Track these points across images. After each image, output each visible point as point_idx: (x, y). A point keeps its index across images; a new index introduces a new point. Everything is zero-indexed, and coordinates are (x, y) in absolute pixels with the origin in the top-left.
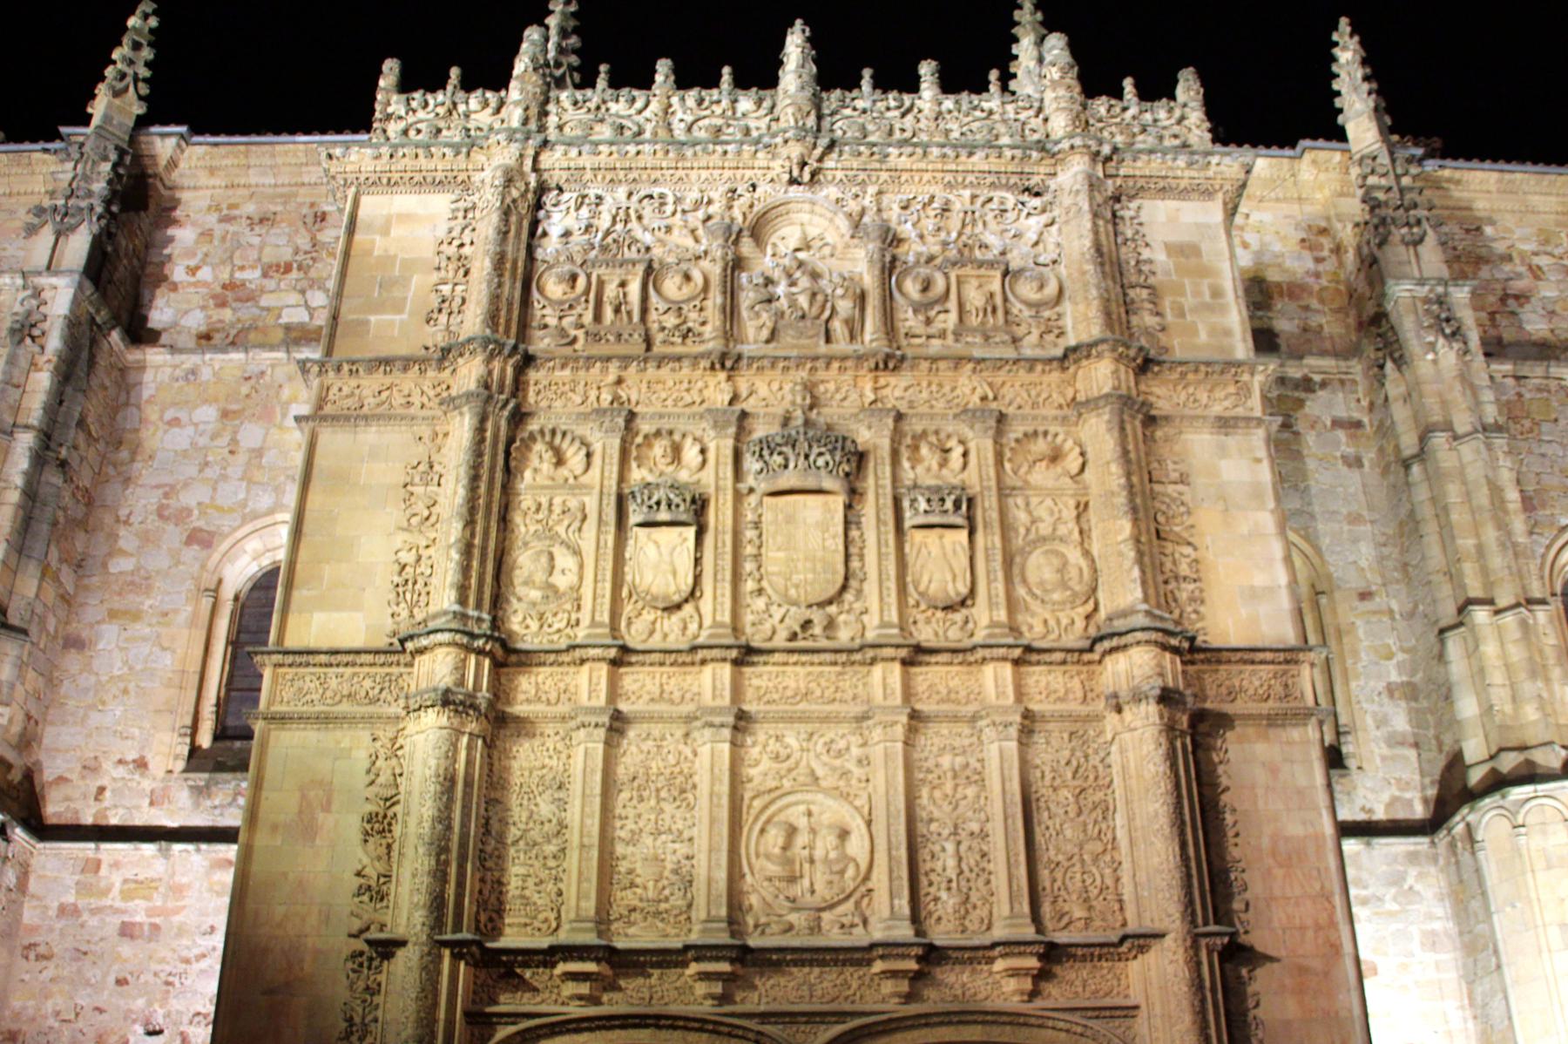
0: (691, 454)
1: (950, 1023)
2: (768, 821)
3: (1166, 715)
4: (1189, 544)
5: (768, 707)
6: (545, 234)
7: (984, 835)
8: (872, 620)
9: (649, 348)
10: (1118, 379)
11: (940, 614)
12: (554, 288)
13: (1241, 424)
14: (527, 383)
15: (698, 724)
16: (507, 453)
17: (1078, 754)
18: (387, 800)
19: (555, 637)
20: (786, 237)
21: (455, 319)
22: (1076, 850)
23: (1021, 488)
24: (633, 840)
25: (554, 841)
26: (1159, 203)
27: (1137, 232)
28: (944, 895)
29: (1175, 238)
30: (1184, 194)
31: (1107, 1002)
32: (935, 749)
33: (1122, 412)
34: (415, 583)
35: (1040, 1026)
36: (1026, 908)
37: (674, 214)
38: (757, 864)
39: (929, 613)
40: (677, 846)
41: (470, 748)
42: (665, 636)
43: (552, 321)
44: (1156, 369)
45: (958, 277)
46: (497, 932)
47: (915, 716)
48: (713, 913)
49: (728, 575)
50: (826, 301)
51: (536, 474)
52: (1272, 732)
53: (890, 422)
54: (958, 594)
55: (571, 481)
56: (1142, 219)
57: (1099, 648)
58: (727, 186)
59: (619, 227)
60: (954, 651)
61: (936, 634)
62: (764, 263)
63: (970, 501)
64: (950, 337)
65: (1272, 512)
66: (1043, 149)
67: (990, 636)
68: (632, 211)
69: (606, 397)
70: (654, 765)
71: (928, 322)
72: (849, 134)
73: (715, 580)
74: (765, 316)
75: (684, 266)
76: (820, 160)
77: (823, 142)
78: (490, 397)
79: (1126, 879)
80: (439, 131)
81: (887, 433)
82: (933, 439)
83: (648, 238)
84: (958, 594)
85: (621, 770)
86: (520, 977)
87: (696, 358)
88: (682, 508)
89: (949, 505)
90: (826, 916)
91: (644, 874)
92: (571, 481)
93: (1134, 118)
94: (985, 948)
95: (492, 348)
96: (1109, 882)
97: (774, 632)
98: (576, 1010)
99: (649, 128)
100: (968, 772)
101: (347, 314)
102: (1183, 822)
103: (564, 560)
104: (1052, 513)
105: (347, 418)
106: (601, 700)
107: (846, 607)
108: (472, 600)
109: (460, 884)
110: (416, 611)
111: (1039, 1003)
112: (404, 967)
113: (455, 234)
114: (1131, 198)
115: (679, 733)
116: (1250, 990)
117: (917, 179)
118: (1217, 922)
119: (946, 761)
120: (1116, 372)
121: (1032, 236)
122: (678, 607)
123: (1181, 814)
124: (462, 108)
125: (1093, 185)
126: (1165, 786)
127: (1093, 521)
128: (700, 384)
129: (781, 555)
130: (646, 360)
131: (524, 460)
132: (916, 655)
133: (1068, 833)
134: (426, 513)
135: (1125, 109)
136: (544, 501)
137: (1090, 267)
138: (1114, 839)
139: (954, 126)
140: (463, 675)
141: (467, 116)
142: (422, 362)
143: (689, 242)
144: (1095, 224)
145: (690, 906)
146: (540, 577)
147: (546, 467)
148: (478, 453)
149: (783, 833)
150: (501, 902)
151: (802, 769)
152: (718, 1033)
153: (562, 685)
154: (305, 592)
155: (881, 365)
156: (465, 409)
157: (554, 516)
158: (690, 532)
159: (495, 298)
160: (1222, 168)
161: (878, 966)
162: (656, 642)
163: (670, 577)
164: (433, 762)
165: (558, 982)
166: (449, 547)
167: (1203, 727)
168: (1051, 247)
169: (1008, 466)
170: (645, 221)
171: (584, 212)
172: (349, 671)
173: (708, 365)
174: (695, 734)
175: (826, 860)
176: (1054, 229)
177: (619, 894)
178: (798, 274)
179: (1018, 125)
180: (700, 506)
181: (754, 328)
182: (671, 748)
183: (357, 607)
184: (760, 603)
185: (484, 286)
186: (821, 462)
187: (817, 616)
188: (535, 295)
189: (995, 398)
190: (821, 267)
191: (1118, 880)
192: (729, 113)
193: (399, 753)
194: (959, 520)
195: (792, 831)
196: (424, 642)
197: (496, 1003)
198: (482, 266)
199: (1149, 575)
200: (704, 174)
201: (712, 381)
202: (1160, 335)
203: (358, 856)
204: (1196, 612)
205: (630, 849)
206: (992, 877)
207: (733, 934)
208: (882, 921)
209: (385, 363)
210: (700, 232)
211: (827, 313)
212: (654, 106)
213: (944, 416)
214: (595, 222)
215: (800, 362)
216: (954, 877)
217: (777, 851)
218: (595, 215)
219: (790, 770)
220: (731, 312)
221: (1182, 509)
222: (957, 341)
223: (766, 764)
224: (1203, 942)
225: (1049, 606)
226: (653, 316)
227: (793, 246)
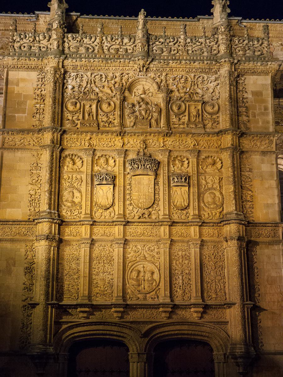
0: (111, 162)
1: (179, 325)
2: (133, 269)
3: (239, 244)
4: (250, 190)
5: (133, 238)
6: (67, 88)
7: (189, 274)
8: (161, 213)
9: (99, 129)
10: (233, 141)
11: (180, 211)
12: (71, 108)
13: (269, 153)
14: (64, 138)
15: (114, 242)
16: (60, 162)
17: (216, 252)
18: (31, 263)
19: (75, 217)
20: (138, 89)
21: (42, 116)
22: (214, 279)
23: (203, 173)
24: (98, 274)
25: (76, 275)
26: (251, 77)
27: (244, 88)
28: (179, 290)
29: (254, 89)
30: (259, 74)
31: (221, 320)
32: (177, 250)
33: (234, 152)
34: (35, 200)
35: (203, 326)
36: (200, 295)
37: (105, 82)
38: (130, 281)
39: (177, 211)
40: (109, 276)
41: (53, 250)
42: (105, 217)
43: (70, 118)
44: (245, 136)
45: (189, 105)
46: (62, 300)
47: (172, 240)
48: (118, 295)
49: (122, 200)
50: (150, 113)
51: (68, 166)
52: (269, 246)
53: (168, 153)
54: (185, 206)
55: (78, 170)
56: (245, 83)
57: (222, 224)
58: (121, 72)
59: (89, 85)
60: (183, 223)
61: (179, 217)
62: (133, 99)
63: (189, 177)
64: (186, 125)
65: (275, 180)
66: (216, 61)
67: (193, 219)
68: (92, 80)
69: (87, 144)
70: (102, 254)
71: (180, 119)
72: (158, 51)
73: (119, 201)
74: (132, 118)
75: (109, 101)
76: (149, 64)
77: (150, 60)
78: (55, 146)
79: (226, 287)
80: (31, 47)
81: (166, 157)
82: (179, 158)
83: (97, 90)
84: (185, 206)
85: (94, 255)
86: (68, 312)
87: (112, 132)
88: (109, 180)
89: (183, 180)
90: (148, 295)
91: (101, 283)
92: (78, 170)
93: (246, 44)
94: (189, 305)
95: (54, 129)
96: (222, 287)
97: (135, 216)
98: (83, 321)
99: (96, 48)
100: (186, 256)
101: (9, 114)
102: (242, 273)
103: (77, 194)
104: (212, 182)
105: (12, 149)
106: (88, 236)
107: (154, 209)
108: (52, 208)
109: (53, 288)
110: (36, 208)
111: (203, 320)
112: (39, 310)
113: (39, 87)
114: (243, 75)
115: (109, 245)
116: (259, 318)
117: (178, 70)
118: (250, 300)
119: (180, 253)
120: (233, 139)
121: (211, 90)
122: (109, 208)
123: (242, 271)
124: (37, 39)
125: (231, 74)
126: (238, 263)
127: (224, 184)
128: (114, 140)
129: (137, 194)
130: (98, 133)
131: (64, 163)
132: (173, 224)
133: (212, 274)
134: (37, 179)
135: (244, 41)
136: (70, 176)
137: (227, 103)
138: (224, 276)
139: (190, 48)
140: (51, 230)
141: (39, 42)
142: (33, 131)
143: (110, 92)
144: (230, 88)
145: (112, 292)
146: (70, 199)
147: (71, 165)
148: (52, 163)
149: (137, 273)
150: (63, 292)
151: (142, 255)
152: (120, 327)
153: (77, 231)
154: (3, 202)
155: (165, 135)
156: (47, 149)
157: (73, 181)
158: (112, 187)
159: (54, 113)
160: (272, 65)
161: (161, 309)
162: (102, 219)
163: (107, 200)
164: (44, 255)
165: (78, 313)
166: (46, 191)
167: (250, 245)
168: (217, 94)
169: (200, 167)
170: (96, 84)
171: (78, 79)
172: (18, 226)
173: (116, 135)
174: (114, 245)
175: (148, 280)
176: (219, 86)
177: (94, 289)
178: (142, 103)
179: (209, 48)
180: (114, 178)
181: (129, 122)
182: (107, 249)
183: (19, 207)
184: (132, 207)
185: (50, 108)
186: (148, 167)
187: (146, 212)
188: (65, 109)
189: (198, 145)
190: (148, 100)
191: (225, 287)
192: (121, 44)
193: (34, 250)
194: (186, 184)
195: (139, 272)
196: (40, 221)
197: (62, 319)
198: (49, 101)
199: (238, 202)
200: (114, 68)
201: (117, 139)
202: (247, 123)
203: (24, 279)
204: (251, 211)
205: (97, 277)
206: (191, 286)
207: (124, 301)
208: (162, 297)
209: (22, 131)
210: (113, 88)
211: (150, 117)
212: (98, 40)
213: (183, 151)
214: (82, 83)
215: (142, 134)
216: (181, 285)
217: (135, 277)
218: (82, 81)
219: (139, 255)
220: (122, 116)
221: (250, 180)
222: (187, 127)
223: (132, 253)
224: (246, 306)
225: (210, 209)
226: (100, 117)
227: (140, 93)
